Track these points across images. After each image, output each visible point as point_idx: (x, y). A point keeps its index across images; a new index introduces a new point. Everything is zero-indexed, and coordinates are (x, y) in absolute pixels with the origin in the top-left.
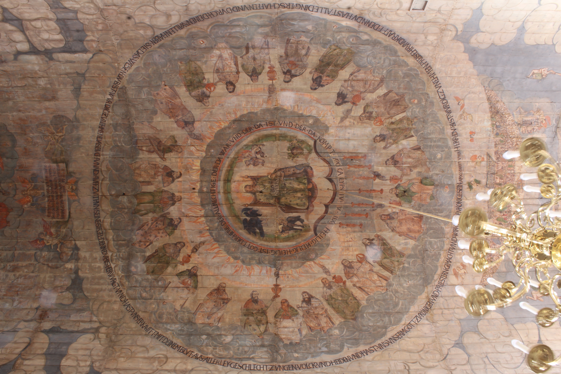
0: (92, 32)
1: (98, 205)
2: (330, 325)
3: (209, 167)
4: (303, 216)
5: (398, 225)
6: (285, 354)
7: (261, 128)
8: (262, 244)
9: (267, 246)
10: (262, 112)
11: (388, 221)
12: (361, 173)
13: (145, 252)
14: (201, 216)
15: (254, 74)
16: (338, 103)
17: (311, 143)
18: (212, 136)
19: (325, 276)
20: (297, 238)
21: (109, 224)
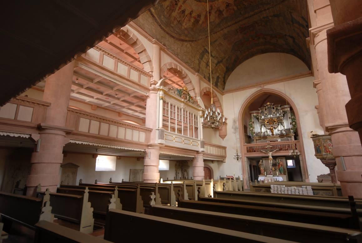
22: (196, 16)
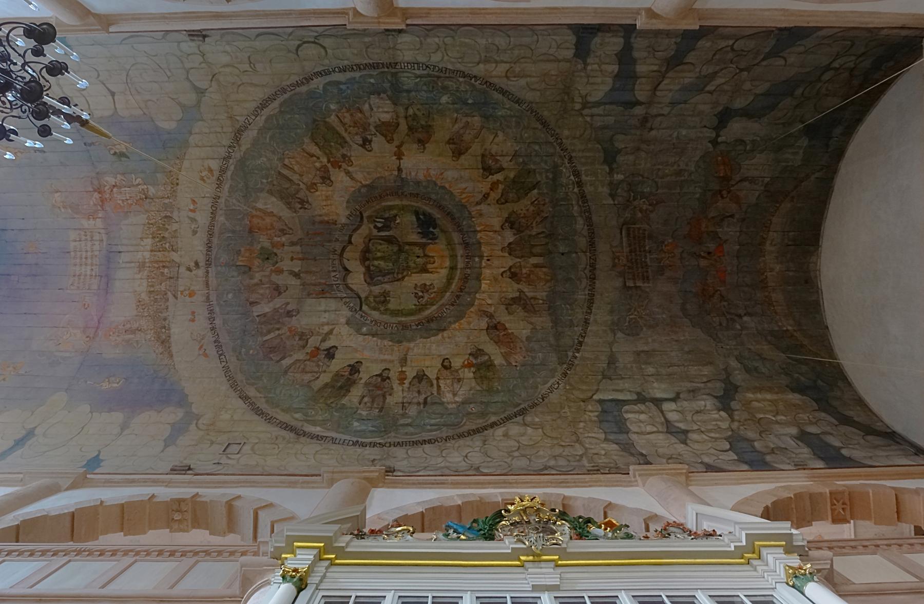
0: (591, 421)
1: (590, 242)
2: (340, 115)
4: (375, 232)
5: (275, 223)
6: (384, 82)
7: (417, 323)
8: (417, 202)
9: (411, 201)
11: (285, 228)
12: (314, 278)
13: (539, 194)
14: (480, 231)
15: (420, 377)
17: (365, 308)
19: (350, 169)
22: (468, 359)
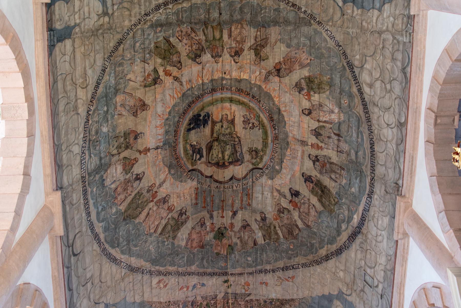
3: (243, 86)
4: (203, 159)
7: (273, 129)
10: (285, 132)
15: (317, 133)
16: (292, 190)
18: (268, 90)
20: (186, 158)
21: (196, 2)
